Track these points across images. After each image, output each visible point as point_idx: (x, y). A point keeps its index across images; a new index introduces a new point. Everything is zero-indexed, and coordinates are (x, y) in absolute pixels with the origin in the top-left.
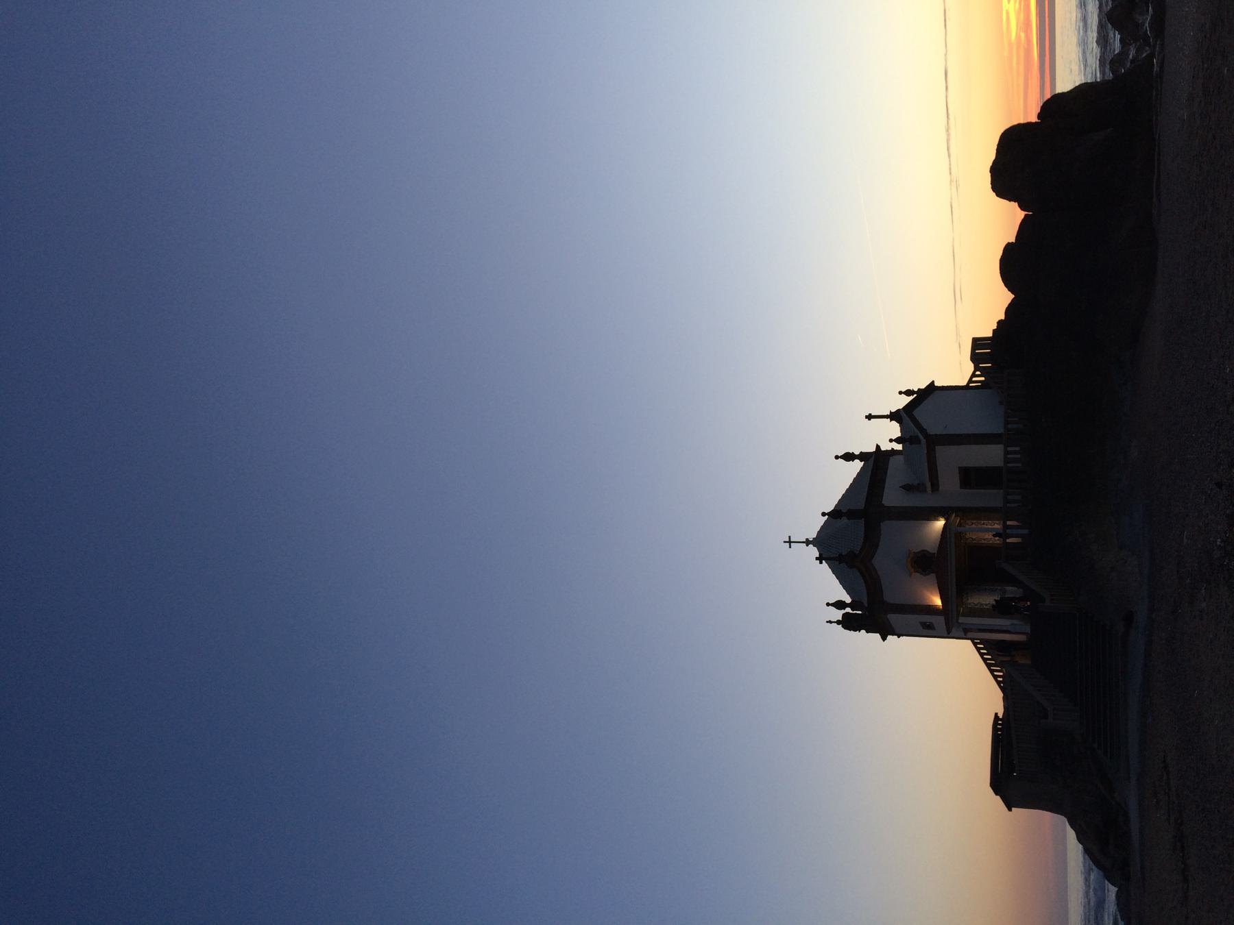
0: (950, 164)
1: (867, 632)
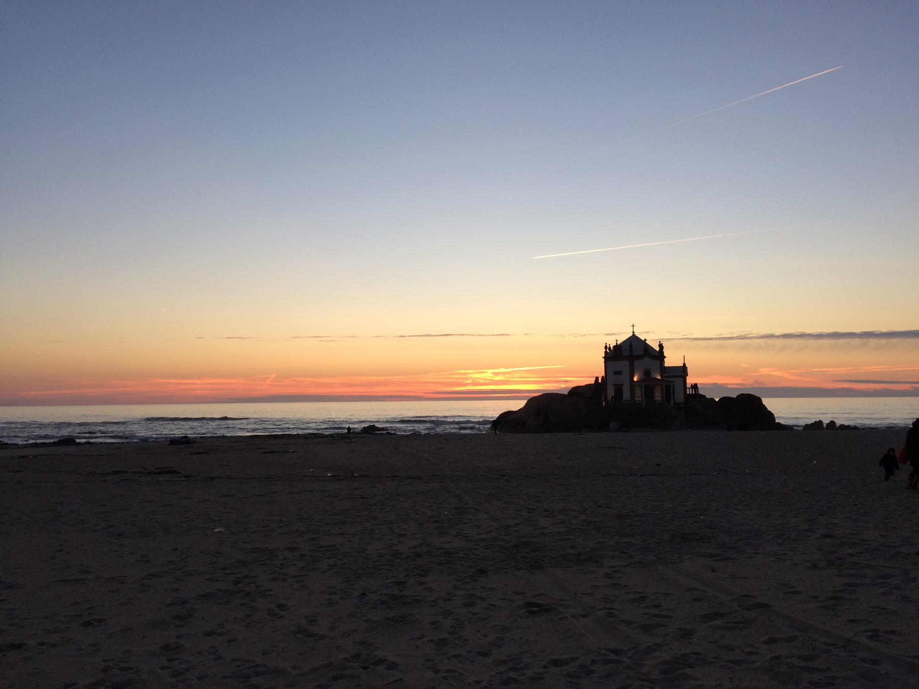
0: (433, 336)
1: (605, 352)
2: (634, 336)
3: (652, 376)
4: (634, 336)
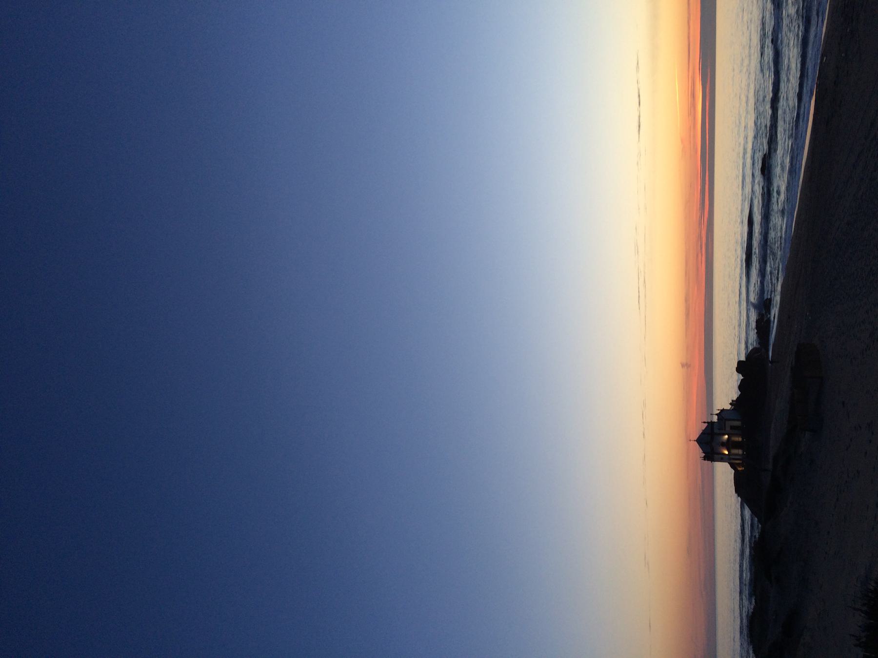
2: (696, 441)
3: (724, 441)
4: (696, 441)
